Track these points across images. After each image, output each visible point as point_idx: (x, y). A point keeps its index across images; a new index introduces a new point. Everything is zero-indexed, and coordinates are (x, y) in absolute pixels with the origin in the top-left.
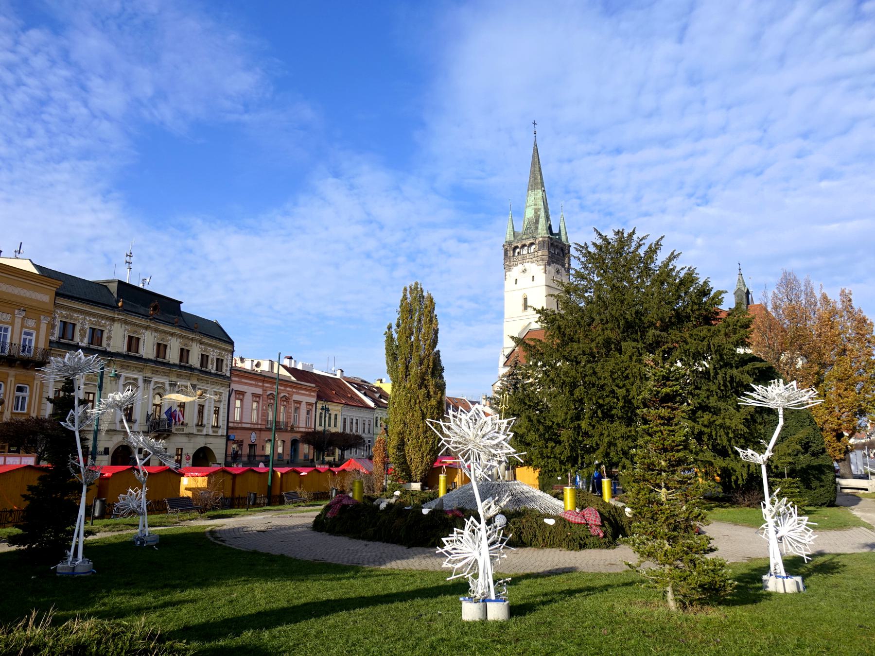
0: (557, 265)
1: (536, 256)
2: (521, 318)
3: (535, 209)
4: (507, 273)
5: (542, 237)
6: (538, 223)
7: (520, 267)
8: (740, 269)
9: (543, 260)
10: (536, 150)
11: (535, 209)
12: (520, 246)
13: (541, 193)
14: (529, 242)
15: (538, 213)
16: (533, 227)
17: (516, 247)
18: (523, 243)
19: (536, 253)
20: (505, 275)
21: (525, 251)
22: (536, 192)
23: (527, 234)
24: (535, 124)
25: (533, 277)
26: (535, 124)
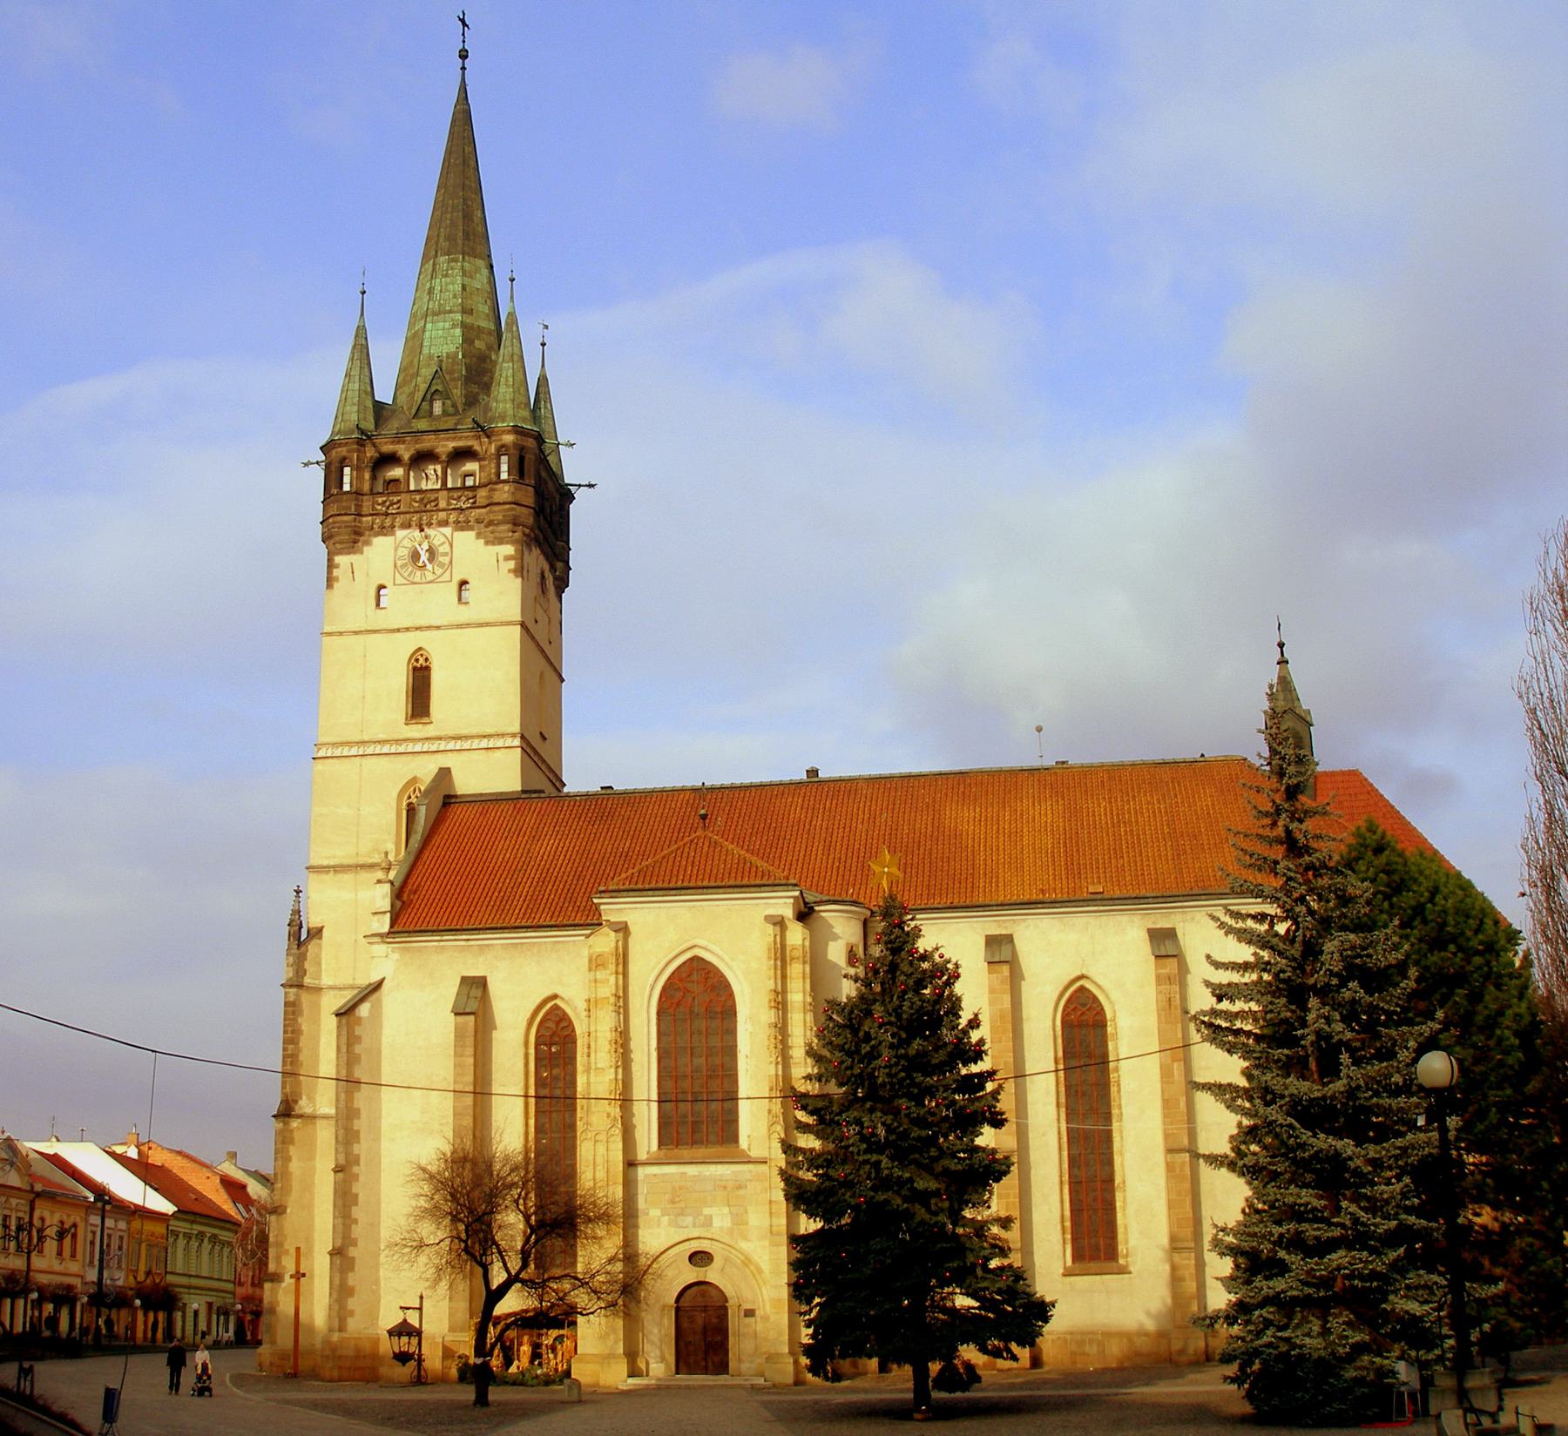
0: (541, 557)
1: (481, 501)
2: (401, 749)
3: (463, 325)
4: (338, 559)
5: (517, 430)
7: (406, 538)
8: (1281, 645)
9: (515, 523)
10: (463, 119)
12: (406, 457)
13: (485, 272)
14: (451, 445)
15: (477, 344)
16: (458, 392)
17: (391, 459)
18: (427, 443)
19: (482, 493)
20: (331, 565)
21: (430, 478)
22: (465, 264)
24: (463, 21)
26: (464, 24)
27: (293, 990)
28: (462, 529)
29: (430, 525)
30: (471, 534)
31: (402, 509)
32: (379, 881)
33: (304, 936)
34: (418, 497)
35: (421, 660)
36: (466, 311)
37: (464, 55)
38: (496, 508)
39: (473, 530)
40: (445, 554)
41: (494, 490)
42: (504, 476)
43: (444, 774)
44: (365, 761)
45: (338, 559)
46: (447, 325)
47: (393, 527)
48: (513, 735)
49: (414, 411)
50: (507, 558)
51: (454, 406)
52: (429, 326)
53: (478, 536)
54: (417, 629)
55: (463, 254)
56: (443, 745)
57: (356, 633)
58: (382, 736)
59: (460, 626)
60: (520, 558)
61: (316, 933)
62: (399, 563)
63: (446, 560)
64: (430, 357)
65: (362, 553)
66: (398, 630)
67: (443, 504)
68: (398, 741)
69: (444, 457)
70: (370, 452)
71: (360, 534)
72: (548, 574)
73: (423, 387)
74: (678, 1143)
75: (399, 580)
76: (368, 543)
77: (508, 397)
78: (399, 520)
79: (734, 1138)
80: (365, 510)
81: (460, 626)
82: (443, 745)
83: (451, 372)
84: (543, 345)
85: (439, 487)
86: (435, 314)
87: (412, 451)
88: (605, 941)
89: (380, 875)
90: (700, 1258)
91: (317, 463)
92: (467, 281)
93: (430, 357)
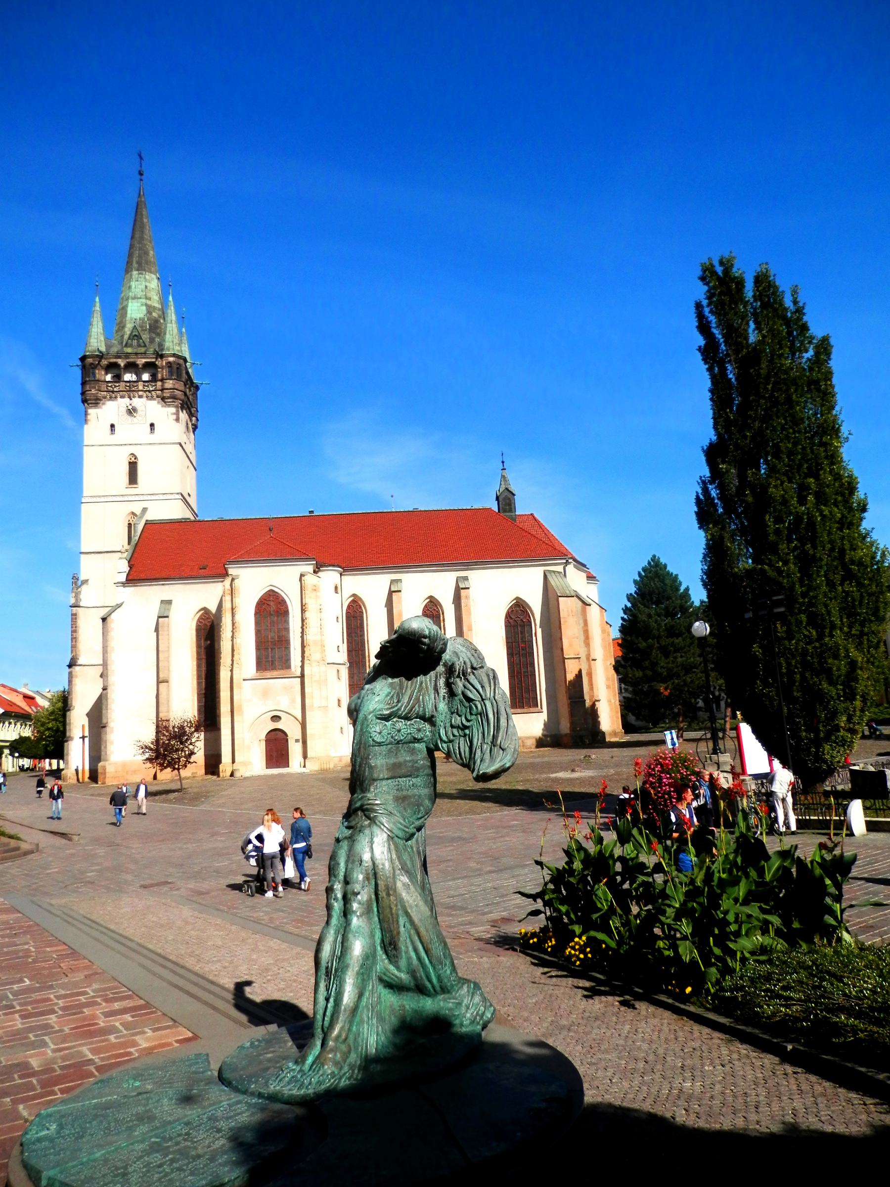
2: (126, 498)
3: (146, 305)
4: (90, 411)
5: (174, 355)
9: (174, 397)
11: (146, 305)
12: (122, 365)
13: (156, 281)
14: (144, 360)
18: (132, 360)
19: (159, 384)
20: (86, 414)
23: (131, 346)
25: (152, 425)
26: (141, 158)
27: (74, 609)
28: (150, 400)
29: (134, 397)
31: (121, 389)
32: (121, 558)
33: (79, 583)
34: (128, 384)
35: (133, 459)
37: (141, 174)
39: (155, 400)
43: (145, 510)
45: (90, 411)
46: (139, 304)
47: (116, 397)
48: (178, 494)
49: (124, 344)
50: (174, 414)
51: (144, 342)
52: (130, 304)
53: (158, 402)
55: (145, 270)
56: (145, 498)
60: (177, 414)
61: (85, 582)
62: (120, 414)
63: (143, 414)
64: (131, 319)
65: (100, 407)
69: (140, 366)
70: (104, 362)
71: (100, 400)
72: (189, 422)
73: (128, 333)
74: (265, 669)
76: (104, 404)
77: (170, 340)
79: (289, 667)
82: (145, 498)
83: (141, 327)
88: (228, 581)
89: (119, 555)
90: (275, 718)
91: (78, 366)
93: (131, 319)
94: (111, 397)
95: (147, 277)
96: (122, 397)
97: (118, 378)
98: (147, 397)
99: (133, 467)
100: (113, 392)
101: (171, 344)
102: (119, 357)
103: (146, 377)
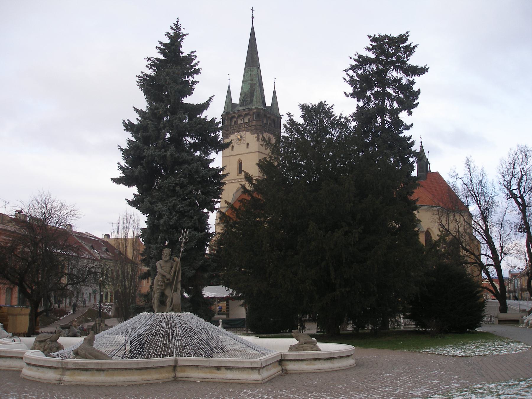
1: (250, 125)
2: (236, 181)
3: (250, 84)
6: (253, 97)
9: (256, 129)
12: (236, 116)
13: (256, 70)
14: (245, 113)
15: (254, 87)
16: (249, 100)
19: (250, 123)
22: (252, 69)
25: (248, 144)
26: (252, 10)
29: (241, 131)
30: (249, 132)
34: (238, 125)
36: (251, 80)
37: (253, 17)
38: (253, 127)
40: (244, 137)
41: (252, 123)
42: (255, 119)
44: (230, 184)
46: (247, 84)
47: (234, 132)
48: (257, 177)
51: (248, 103)
53: (250, 133)
54: (239, 154)
57: (228, 156)
58: (233, 178)
59: (247, 153)
60: (258, 137)
66: (235, 155)
67: (243, 126)
68: (236, 179)
70: (230, 116)
75: (236, 144)
76: (230, 136)
78: (235, 131)
80: (229, 129)
81: (247, 153)
84: (274, 83)
85: (242, 122)
86: (245, 82)
87: (237, 115)
92: (251, 73)
94: (232, 133)
95: (252, 69)
96: (237, 132)
97: (236, 123)
98: (246, 130)
99: (240, 165)
100: (233, 130)
101: (255, 103)
102: (235, 113)
103: (246, 120)
